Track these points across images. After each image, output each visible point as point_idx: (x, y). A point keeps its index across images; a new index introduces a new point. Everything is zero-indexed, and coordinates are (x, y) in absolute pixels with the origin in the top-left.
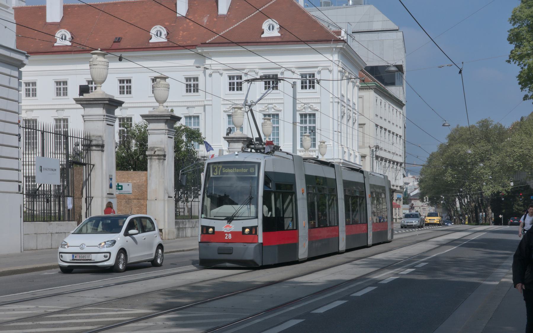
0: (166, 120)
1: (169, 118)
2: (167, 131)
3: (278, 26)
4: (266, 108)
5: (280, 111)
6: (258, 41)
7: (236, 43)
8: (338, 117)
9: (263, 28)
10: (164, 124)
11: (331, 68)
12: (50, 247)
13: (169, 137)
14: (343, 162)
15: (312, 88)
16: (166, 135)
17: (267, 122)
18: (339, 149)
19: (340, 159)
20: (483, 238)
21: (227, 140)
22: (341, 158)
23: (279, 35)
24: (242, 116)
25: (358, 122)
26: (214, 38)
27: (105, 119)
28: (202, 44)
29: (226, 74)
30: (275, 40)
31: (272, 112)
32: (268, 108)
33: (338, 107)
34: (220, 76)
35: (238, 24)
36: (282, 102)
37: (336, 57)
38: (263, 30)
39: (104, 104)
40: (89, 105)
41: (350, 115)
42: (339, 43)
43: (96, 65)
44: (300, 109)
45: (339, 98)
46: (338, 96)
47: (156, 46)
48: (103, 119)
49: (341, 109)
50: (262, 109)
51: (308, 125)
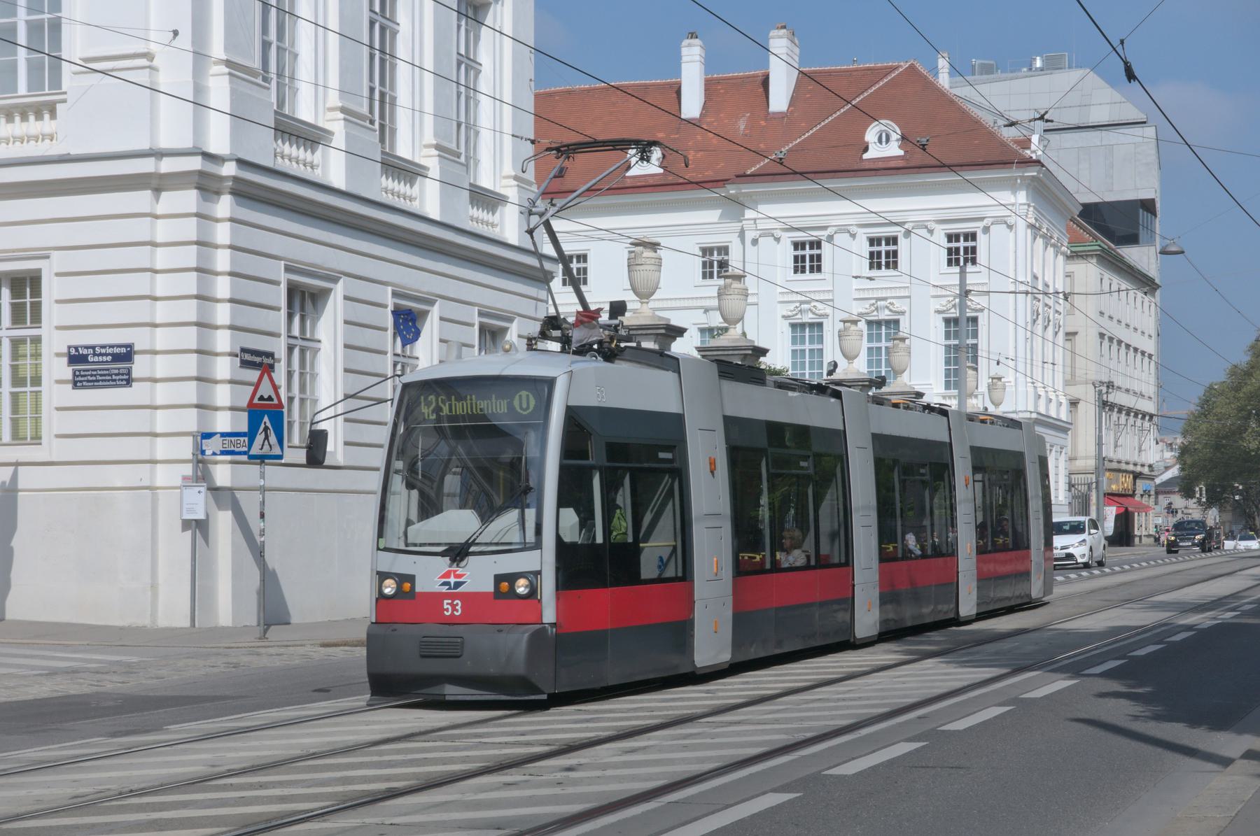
0: (742, 356)
1: (750, 352)
4: (873, 308)
5: (903, 313)
8: (1027, 323)
17: (898, 344)
18: (1027, 391)
19: (1031, 412)
22: (1033, 410)
24: (859, 337)
29: (787, 239)
31: (885, 315)
32: (877, 309)
36: (907, 294)
39: (657, 334)
41: (1049, 317)
44: (945, 308)
47: (639, 184)
49: (1032, 306)
50: (864, 311)
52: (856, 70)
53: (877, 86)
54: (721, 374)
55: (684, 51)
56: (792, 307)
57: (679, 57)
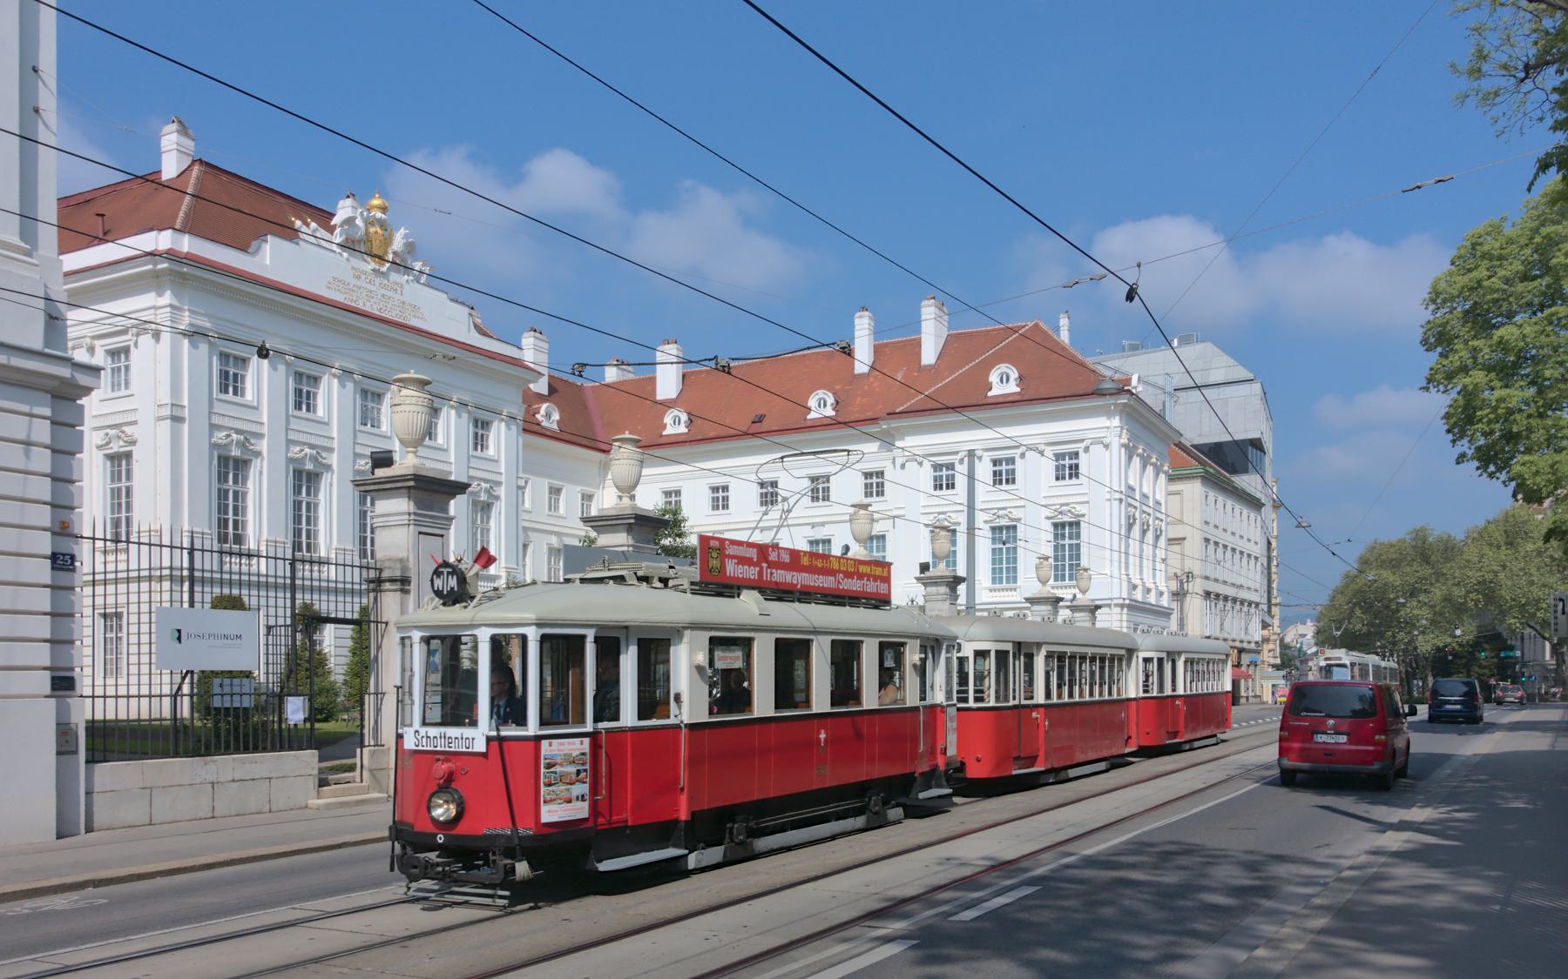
1: (632, 521)
3: (1017, 375)
5: (1019, 520)
6: (980, 403)
7: (952, 408)
8: (1120, 526)
10: (625, 534)
11: (1106, 441)
12: (210, 815)
23: (1018, 390)
30: (1010, 399)
31: (1004, 522)
37: (1116, 421)
39: (409, 487)
45: (1121, 492)
46: (1120, 486)
48: (406, 522)
49: (1127, 512)
51: (1067, 542)
52: (993, 330)
55: (857, 321)
57: (854, 327)
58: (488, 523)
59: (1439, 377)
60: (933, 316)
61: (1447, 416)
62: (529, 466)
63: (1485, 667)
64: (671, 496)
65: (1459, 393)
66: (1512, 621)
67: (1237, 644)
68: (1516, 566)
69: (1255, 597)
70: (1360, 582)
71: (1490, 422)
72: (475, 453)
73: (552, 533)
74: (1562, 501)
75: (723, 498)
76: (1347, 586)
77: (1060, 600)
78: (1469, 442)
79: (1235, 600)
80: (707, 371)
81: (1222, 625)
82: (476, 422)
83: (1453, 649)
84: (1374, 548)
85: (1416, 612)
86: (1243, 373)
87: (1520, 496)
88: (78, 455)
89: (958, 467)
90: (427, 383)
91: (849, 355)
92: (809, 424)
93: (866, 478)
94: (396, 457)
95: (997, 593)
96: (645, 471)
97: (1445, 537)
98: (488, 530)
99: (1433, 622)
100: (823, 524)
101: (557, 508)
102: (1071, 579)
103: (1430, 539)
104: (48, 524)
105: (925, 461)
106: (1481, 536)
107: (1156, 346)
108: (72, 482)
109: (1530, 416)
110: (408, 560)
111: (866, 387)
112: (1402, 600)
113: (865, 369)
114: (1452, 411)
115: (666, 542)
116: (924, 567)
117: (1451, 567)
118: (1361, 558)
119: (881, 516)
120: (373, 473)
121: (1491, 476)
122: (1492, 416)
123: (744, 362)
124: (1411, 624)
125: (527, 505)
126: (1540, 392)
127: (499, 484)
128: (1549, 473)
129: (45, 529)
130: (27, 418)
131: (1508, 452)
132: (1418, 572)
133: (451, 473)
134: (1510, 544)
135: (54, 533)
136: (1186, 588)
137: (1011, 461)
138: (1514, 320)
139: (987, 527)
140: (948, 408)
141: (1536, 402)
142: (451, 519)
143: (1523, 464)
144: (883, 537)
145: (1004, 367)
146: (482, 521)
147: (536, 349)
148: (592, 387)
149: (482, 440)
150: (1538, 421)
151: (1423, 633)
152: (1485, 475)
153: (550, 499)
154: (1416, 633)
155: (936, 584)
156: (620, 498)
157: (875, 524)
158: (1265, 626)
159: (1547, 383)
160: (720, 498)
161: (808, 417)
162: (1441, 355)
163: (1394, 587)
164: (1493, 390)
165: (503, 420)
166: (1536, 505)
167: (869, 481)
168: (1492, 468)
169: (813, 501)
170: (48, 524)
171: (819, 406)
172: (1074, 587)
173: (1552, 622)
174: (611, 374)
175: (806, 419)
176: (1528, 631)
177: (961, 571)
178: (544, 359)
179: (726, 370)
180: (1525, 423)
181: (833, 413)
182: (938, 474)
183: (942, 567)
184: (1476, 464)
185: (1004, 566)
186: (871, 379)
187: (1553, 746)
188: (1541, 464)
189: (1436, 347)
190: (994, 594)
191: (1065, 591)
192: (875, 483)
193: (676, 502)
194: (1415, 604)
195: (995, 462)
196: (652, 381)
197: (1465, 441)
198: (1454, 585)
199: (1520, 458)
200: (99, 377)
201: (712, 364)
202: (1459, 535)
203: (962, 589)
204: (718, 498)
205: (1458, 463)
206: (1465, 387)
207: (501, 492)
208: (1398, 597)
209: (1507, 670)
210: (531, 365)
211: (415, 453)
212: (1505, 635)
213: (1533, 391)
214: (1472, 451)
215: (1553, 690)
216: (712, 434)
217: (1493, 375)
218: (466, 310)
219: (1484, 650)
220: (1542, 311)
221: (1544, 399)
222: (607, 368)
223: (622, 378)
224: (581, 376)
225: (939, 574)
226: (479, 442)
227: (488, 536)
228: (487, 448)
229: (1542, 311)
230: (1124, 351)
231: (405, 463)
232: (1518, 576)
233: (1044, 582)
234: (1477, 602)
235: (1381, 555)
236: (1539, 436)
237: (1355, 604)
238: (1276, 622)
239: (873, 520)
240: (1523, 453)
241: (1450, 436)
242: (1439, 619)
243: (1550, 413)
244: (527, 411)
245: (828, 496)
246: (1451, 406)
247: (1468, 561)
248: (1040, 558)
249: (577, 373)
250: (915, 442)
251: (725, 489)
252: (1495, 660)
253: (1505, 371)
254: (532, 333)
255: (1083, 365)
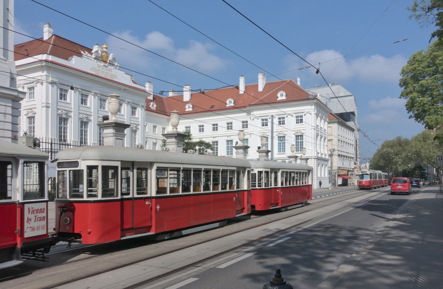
1: (177, 135)
2: (176, 143)
3: (285, 94)
7: (267, 103)
8: (314, 136)
9: (278, 96)
10: (174, 139)
11: (310, 112)
13: (178, 146)
14: (317, 158)
15: (301, 123)
16: (176, 145)
19: (315, 157)
20: (378, 199)
21: (235, 148)
23: (286, 98)
25: (327, 138)
26: (255, 102)
27: (114, 136)
28: (249, 105)
33: (314, 131)
34: (257, 120)
35: (267, 95)
37: (313, 107)
38: (278, 97)
39: (113, 126)
40: (105, 127)
41: (322, 135)
42: (315, 100)
43: (111, 103)
45: (315, 127)
46: (314, 125)
48: (113, 136)
49: (316, 132)
50: (277, 134)
51: (299, 141)
52: (279, 82)
53: (282, 85)
54: (124, 137)
56: (261, 134)
58: (136, 136)
59: (404, 94)
60: (262, 78)
61: (406, 105)
62: (147, 120)
63: (417, 175)
64: (187, 128)
65: (410, 99)
66: (425, 162)
67: (347, 169)
68: (426, 147)
69: (352, 156)
70: (382, 151)
71: (418, 107)
72: (132, 116)
73: (154, 138)
74: (439, 129)
75: (202, 129)
76: (378, 153)
77: (297, 157)
78: (413, 112)
79: (347, 157)
80: (198, 93)
81: (343, 164)
82: (132, 108)
83: (408, 170)
84: (386, 142)
85: (398, 160)
86: (349, 94)
87: (427, 127)
88: (19, 117)
89: (269, 120)
90: (118, 97)
91: (238, 89)
92: (226, 108)
93: (243, 123)
94: (110, 117)
95: (280, 155)
96: (180, 121)
97: (406, 139)
98: (136, 138)
99: (402, 163)
100: (230, 136)
101: (155, 132)
102: (300, 151)
103: (402, 140)
104: (11, 136)
105: (259, 118)
106: (416, 139)
107: (324, 86)
108: (18, 124)
109: (430, 105)
110: (113, 145)
111: (243, 98)
112: (394, 157)
113: (243, 93)
114: (408, 104)
115: (186, 141)
116: (259, 148)
117: (408, 148)
118: (382, 145)
119: (247, 133)
120: (103, 122)
121: (419, 122)
122: (419, 105)
123: (208, 91)
124: (396, 163)
125: (147, 131)
126: (432, 99)
127: (139, 125)
128: (435, 121)
129: (10, 138)
130: (5, 107)
131: (423, 115)
132: (398, 149)
133: (125, 122)
134: (424, 141)
135: (12, 139)
136: (333, 154)
137: (284, 118)
138: (425, 78)
139: (277, 136)
140: (266, 103)
141: (432, 101)
142: (125, 135)
143: (428, 119)
144: (247, 139)
145: (281, 92)
146: (134, 135)
147: (150, 87)
148: (165, 98)
149: (134, 113)
150: (432, 106)
151: (400, 166)
152: (417, 122)
153: (153, 129)
154: (398, 166)
155: (262, 153)
156: (173, 129)
157: (245, 136)
158: (355, 164)
159: (434, 96)
160: (201, 128)
161: (226, 106)
162: (405, 88)
163: (392, 153)
164: (419, 98)
165: (140, 107)
166: (431, 130)
167: (243, 124)
168: (419, 120)
169: (228, 129)
170: (11, 136)
171: (230, 103)
172: (301, 153)
173: (436, 162)
174: (171, 94)
175: (226, 107)
176: (429, 165)
177: (270, 149)
178: (152, 90)
179: (203, 93)
180: (428, 107)
181: (233, 105)
182: (263, 122)
183: (264, 147)
184: (414, 118)
185: (282, 147)
186: (244, 95)
187: (436, 197)
188: (433, 119)
189: (403, 86)
190: (279, 155)
191: (299, 154)
192: (245, 124)
193: (189, 130)
194: (397, 157)
195: (279, 119)
196: (182, 96)
197: (411, 112)
198: (408, 152)
199: (427, 117)
200: (25, 95)
201: (199, 91)
202: (410, 138)
203: (270, 154)
204: (201, 129)
205: (409, 118)
206: (411, 97)
207: (140, 127)
208: (393, 156)
209: (423, 176)
210: (148, 92)
211: (115, 116)
212: (423, 166)
213: (430, 98)
214: (413, 115)
215: (436, 181)
216: (199, 111)
217: (419, 94)
218: (130, 76)
219: (417, 170)
220: (433, 76)
221: (434, 100)
222: (169, 93)
223: (174, 95)
224: (162, 95)
225: (263, 150)
226: (133, 113)
227: (136, 139)
228: (135, 115)
229: (433, 76)
230: (315, 87)
231: (112, 119)
232: (426, 150)
233: (293, 152)
234: (415, 157)
235: (388, 144)
236: (432, 111)
237: (381, 158)
238: (358, 163)
239: (245, 135)
240: (428, 115)
241: (407, 111)
242: (404, 162)
243: (435, 104)
244: (147, 105)
245: (232, 128)
246: (407, 102)
247: (412, 146)
248: (292, 145)
249: (161, 94)
250: (256, 113)
251: (203, 126)
252: (420, 173)
253: (423, 93)
254: (148, 83)
255: (304, 91)
